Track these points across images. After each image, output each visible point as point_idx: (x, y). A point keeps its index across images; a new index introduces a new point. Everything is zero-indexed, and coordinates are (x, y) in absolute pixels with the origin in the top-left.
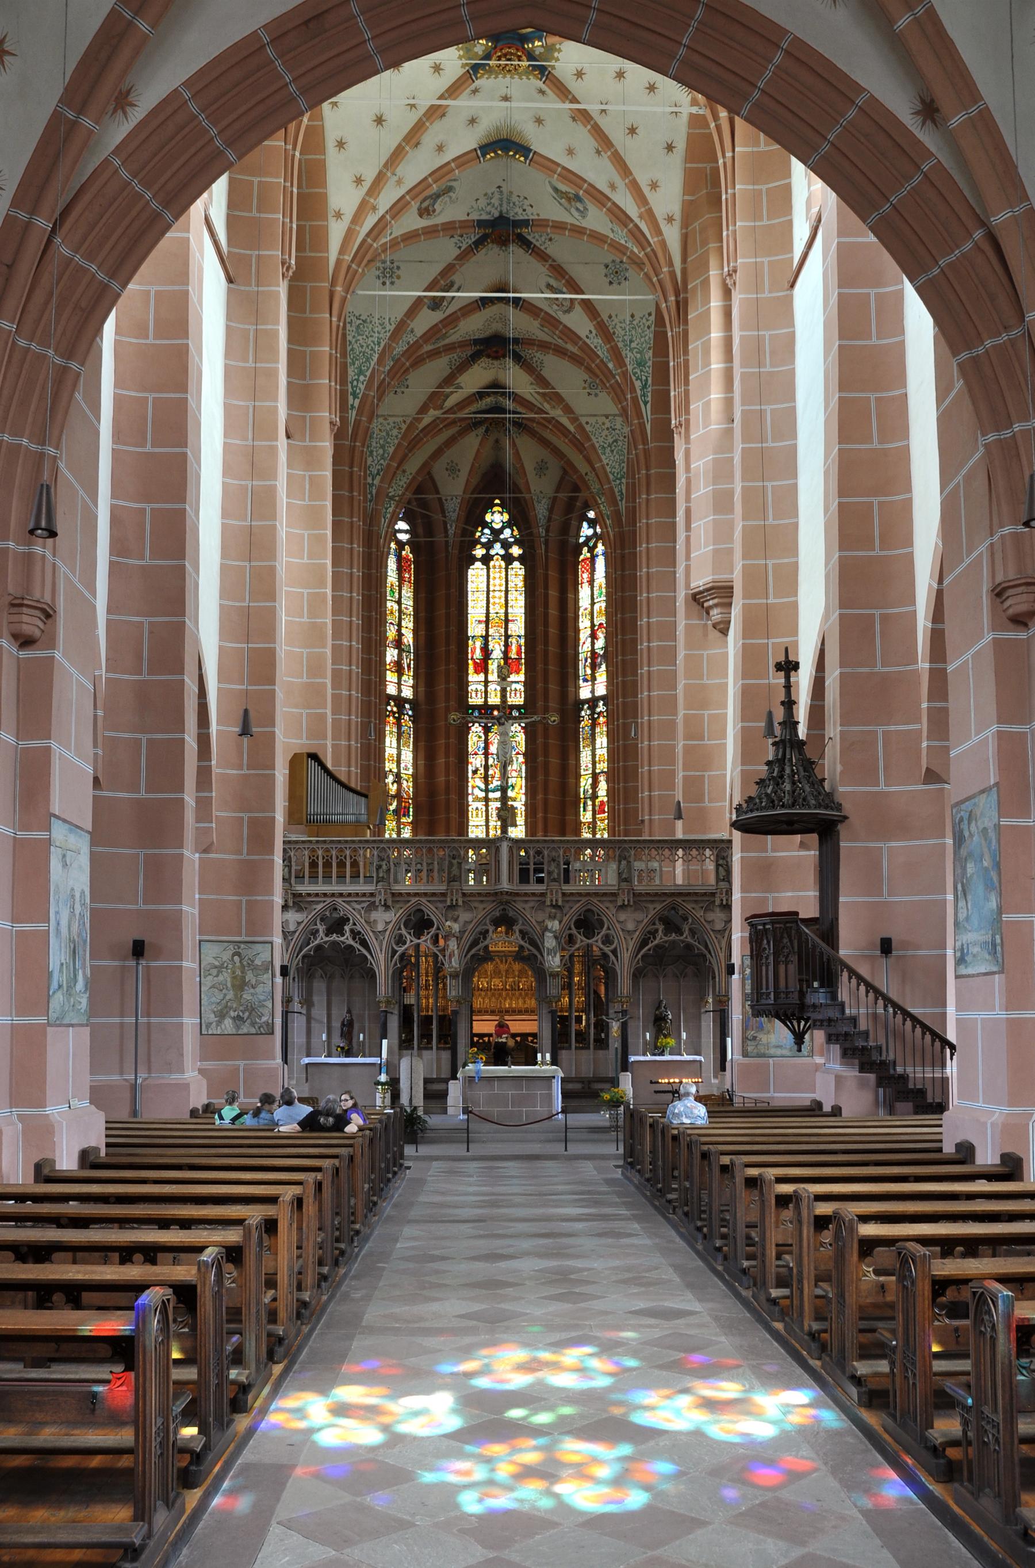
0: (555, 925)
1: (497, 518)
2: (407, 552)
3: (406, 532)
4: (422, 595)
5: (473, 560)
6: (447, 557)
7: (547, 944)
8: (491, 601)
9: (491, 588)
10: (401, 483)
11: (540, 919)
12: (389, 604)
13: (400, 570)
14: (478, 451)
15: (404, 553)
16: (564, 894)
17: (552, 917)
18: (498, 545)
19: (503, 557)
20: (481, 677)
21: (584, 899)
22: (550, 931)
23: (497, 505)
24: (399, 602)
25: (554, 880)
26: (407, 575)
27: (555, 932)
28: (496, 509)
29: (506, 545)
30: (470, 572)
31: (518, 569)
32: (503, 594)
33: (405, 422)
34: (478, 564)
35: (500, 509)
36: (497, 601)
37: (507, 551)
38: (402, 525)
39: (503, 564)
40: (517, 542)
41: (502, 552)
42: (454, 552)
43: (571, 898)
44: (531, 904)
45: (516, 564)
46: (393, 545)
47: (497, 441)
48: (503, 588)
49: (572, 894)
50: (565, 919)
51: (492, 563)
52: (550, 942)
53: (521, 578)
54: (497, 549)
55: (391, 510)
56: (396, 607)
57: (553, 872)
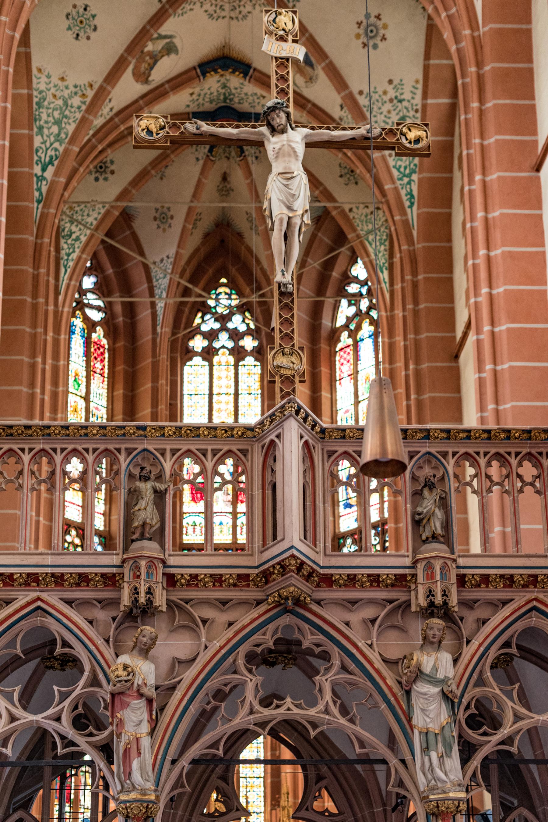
0: (439, 663)
1: (223, 300)
2: (98, 335)
3: (99, 309)
4: (119, 392)
5: (189, 354)
6: (154, 340)
7: (419, 720)
8: (215, 406)
9: (215, 391)
10: (90, 220)
11: (393, 654)
12: (71, 398)
13: (87, 354)
14: (199, 181)
15: (94, 336)
16: (462, 580)
17: (430, 643)
18: (224, 337)
19: (232, 351)
20: (201, 506)
21: (521, 598)
22: (431, 680)
23: (223, 285)
24: (87, 398)
25: (434, 537)
26: (98, 365)
27: (444, 681)
28: (221, 290)
29: (235, 335)
30: (186, 369)
31: (251, 369)
32: (231, 398)
33: (91, 86)
34: (197, 360)
35: (228, 290)
36: (223, 406)
37: (236, 343)
38: (92, 299)
39: (231, 360)
40: (249, 332)
41: (230, 344)
42: (164, 330)
43: (483, 594)
44: (369, 612)
45: (250, 360)
46: (78, 323)
47: (225, 178)
48: (232, 391)
49: (486, 579)
50: (468, 652)
51: (216, 359)
52: (430, 713)
53: (257, 378)
54: (224, 339)
55: (74, 256)
56: (82, 404)
57: (430, 516)
